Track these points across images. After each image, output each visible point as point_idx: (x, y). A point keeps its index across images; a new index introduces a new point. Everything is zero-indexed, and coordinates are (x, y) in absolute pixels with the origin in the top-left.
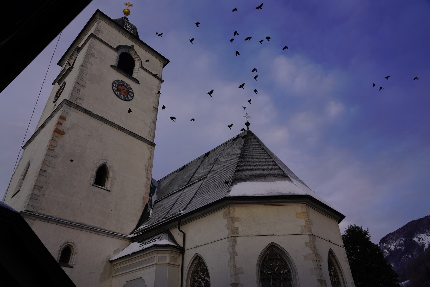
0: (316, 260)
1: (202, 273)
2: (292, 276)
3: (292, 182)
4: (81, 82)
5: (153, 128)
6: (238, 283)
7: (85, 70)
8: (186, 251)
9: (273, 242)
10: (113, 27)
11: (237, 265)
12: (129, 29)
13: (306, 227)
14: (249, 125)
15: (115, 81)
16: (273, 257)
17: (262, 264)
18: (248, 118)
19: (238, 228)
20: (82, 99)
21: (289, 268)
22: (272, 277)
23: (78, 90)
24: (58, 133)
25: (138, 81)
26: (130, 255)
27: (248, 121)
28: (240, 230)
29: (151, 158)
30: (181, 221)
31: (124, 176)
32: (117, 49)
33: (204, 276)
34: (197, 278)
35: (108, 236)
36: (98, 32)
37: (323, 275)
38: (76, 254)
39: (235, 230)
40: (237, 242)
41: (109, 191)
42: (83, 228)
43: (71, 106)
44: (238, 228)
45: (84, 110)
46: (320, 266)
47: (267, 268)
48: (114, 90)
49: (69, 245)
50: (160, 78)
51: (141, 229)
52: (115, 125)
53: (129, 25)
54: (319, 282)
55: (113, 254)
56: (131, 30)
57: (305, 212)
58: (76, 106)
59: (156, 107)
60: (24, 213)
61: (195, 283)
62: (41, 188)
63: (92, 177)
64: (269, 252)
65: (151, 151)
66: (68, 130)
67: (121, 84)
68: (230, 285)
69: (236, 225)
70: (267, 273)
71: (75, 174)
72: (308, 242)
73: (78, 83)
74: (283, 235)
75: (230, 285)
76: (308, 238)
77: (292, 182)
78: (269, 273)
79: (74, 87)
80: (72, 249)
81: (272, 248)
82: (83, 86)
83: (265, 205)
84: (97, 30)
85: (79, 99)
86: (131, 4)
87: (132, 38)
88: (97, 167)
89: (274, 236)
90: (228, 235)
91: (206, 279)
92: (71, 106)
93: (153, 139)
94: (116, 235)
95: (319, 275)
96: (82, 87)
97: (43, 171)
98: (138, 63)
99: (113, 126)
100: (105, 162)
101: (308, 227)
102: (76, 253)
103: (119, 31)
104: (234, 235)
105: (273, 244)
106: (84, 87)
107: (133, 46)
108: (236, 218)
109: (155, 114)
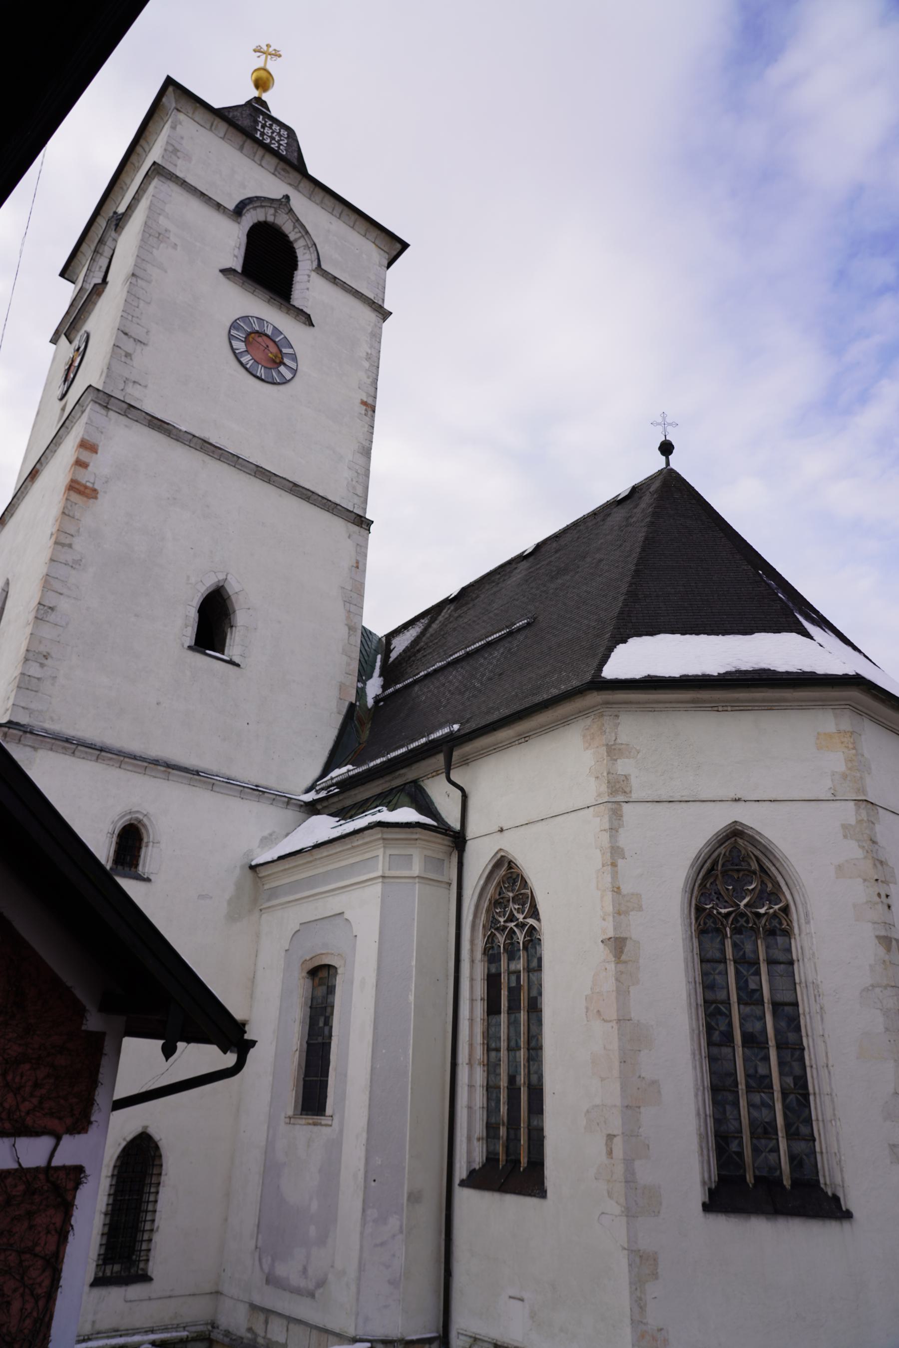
0: (876, 877)
1: (519, 905)
2: (795, 925)
3: (811, 638)
4: (135, 331)
5: (362, 471)
6: (627, 938)
7: (143, 289)
8: (469, 843)
9: (737, 820)
11: (622, 887)
12: (272, 138)
13: (849, 778)
14: (671, 453)
15: (238, 319)
16: (737, 865)
17: (700, 885)
18: (669, 429)
19: (627, 778)
20: (140, 385)
21: (787, 900)
22: (732, 924)
23: (128, 355)
24: (80, 492)
25: (309, 316)
26: (306, 851)
27: (667, 439)
28: (634, 782)
29: (360, 565)
30: (454, 753)
31: (279, 622)
32: (239, 211)
33: (523, 914)
34: (502, 920)
35: (242, 796)
36: (173, 156)
37: (894, 926)
39: (619, 782)
40: (625, 819)
41: (238, 665)
43: (109, 409)
44: (627, 778)
45: (149, 418)
46: (887, 896)
47: (718, 898)
48: (237, 351)
50: (380, 303)
51: (335, 778)
52: (247, 463)
53: (271, 126)
54: (879, 943)
55: (259, 847)
56: (278, 142)
57: (848, 732)
58: (125, 406)
59: (370, 401)
61: (498, 935)
62: (46, 657)
64: (723, 853)
65: (358, 544)
66: (107, 482)
67: (257, 328)
68: (602, 941)
69: (623, 766)
70: (715, 912)
71: (136, 615)
72: (850, 825)
73: (126, 334)
74: (771, 801)
75: (602, 941)
76: (854, 813)
77: (811, 638)
78: (723, 911)
79: (114, 345)
80: (143, 830)
81: (733, 839)
82: (141, 342)
83: (716, 709)
84: (170, 148)
85: (131, 385)
86: (275, 50)
87: (284, 170)
88: (200, 594)
89: (741, 805)
90: (597, 796)
91: (531, 923)
92: (109, 406)
93: (362, 506)
94: (266, 795)
95: (882, 924)
96: (139, 343)
97: (46, 608)
98: (307, 256)
99: (240, 468)
101: (855, 777)
103: (241, 149)
104: (614, 797)
105: (737, 827)
106: (144, 344)
107: (287, 197)
108: (623, 746)
109: (367, 426)
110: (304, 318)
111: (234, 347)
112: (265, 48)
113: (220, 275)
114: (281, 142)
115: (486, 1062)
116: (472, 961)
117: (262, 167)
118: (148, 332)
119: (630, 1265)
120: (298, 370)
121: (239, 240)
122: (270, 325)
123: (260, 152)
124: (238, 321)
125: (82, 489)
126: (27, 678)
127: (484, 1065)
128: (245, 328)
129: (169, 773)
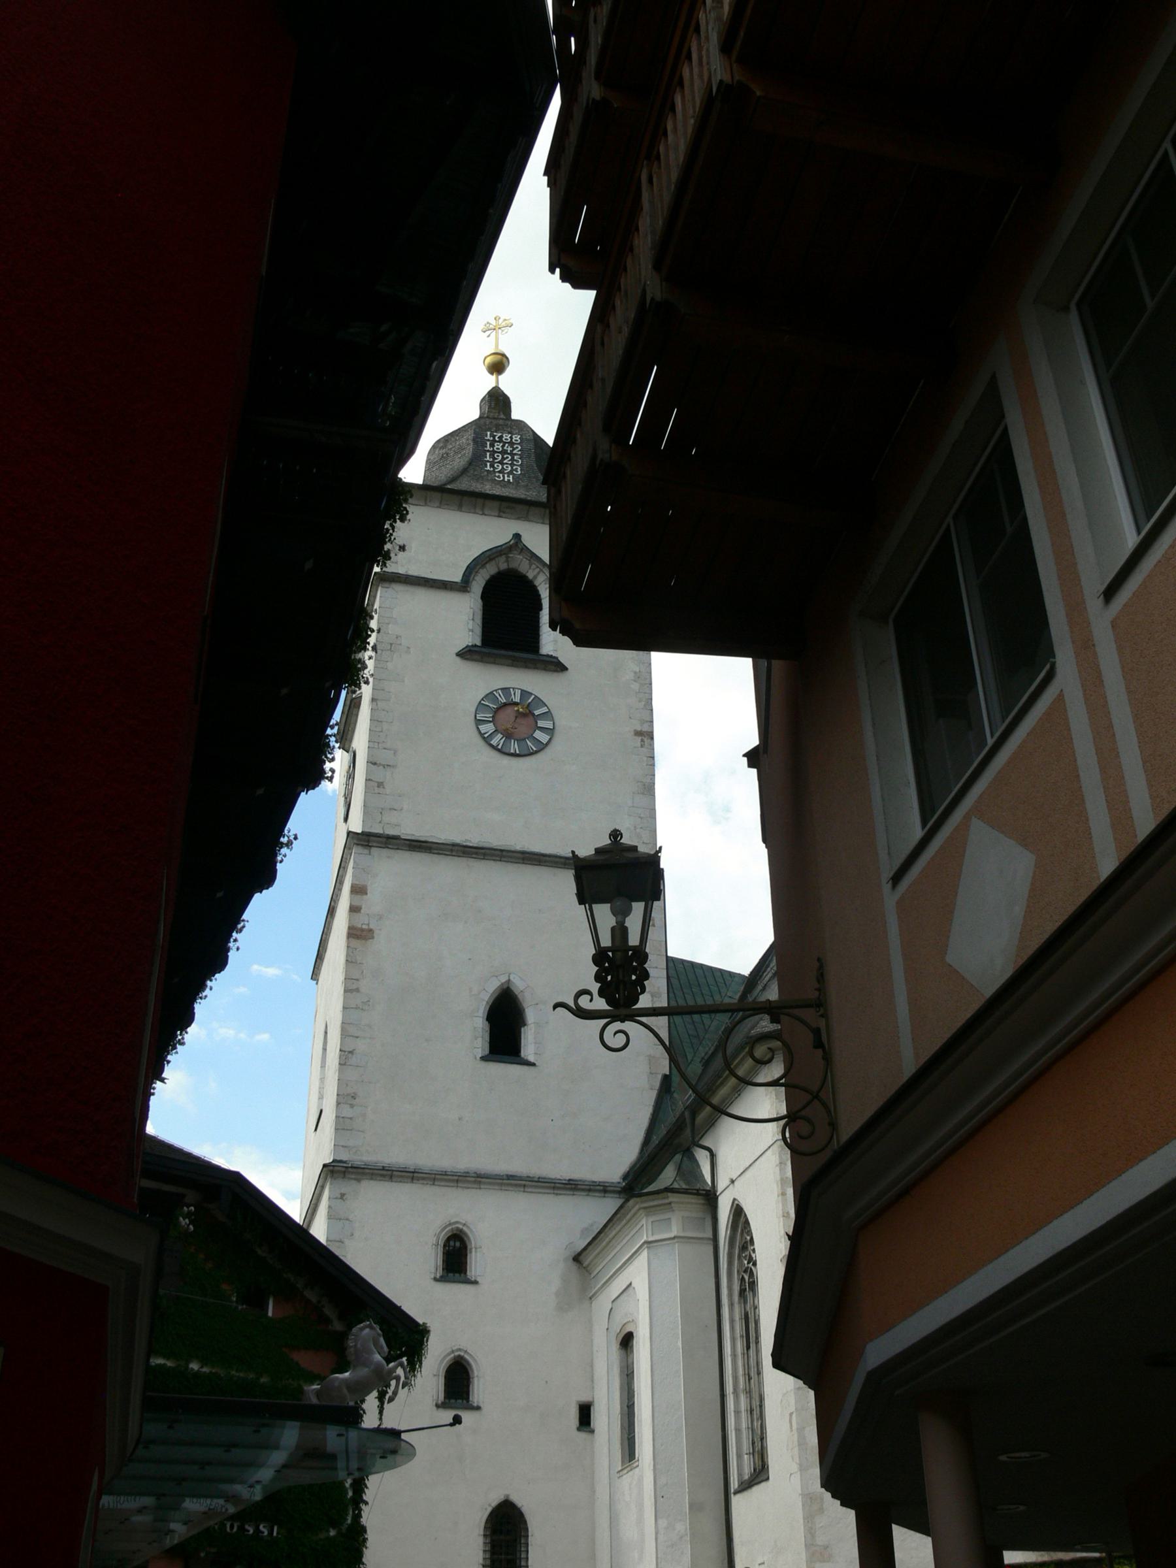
8: (720, 1198)
10: (437, 504)
15: (482, 699)
20: (395, 810)
23: (380, 785)
24: (358, 937)
38: (478, 1250)
41: (533, 1065)
42: (480, 1182)
43: (370, 846)
45: (408, 842)
49: (458, 1229)
59: (645, 728)
60: (331, 1168)
63: (476, 1038)
79: (366, 780)
86: (505, 320)
88: (484, 1003)
92: (370, 844)
97: (346, 1053)
100: (504, 981)
102: (478, 1247)
106: (393, 766)
107: (517, 536)
109: (645, 759)
110: (553, 667)
111: (483, 732)
112: (494, 322)
113: (458, 659)
114: (514, 452)
115: (748, 1390)
116: (731, 1305)
117: (486, 515)
118: (395, 753)
119: (803, 1505)
120: (557, 728)
121: (472, 610)
122: (517, 690)
123: (480, 501)
124: (482, 702)
125: (359, 933)
126: (341, 1120)
127: (746, 1393)
128: (491, 705)
129: (480, 1182)
